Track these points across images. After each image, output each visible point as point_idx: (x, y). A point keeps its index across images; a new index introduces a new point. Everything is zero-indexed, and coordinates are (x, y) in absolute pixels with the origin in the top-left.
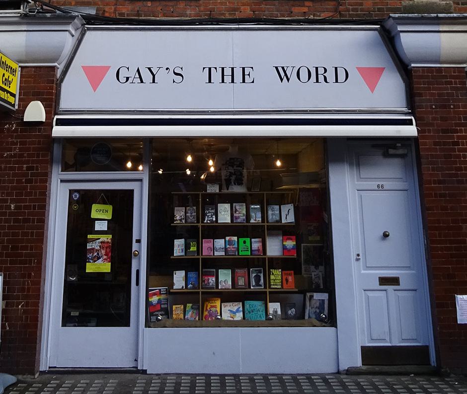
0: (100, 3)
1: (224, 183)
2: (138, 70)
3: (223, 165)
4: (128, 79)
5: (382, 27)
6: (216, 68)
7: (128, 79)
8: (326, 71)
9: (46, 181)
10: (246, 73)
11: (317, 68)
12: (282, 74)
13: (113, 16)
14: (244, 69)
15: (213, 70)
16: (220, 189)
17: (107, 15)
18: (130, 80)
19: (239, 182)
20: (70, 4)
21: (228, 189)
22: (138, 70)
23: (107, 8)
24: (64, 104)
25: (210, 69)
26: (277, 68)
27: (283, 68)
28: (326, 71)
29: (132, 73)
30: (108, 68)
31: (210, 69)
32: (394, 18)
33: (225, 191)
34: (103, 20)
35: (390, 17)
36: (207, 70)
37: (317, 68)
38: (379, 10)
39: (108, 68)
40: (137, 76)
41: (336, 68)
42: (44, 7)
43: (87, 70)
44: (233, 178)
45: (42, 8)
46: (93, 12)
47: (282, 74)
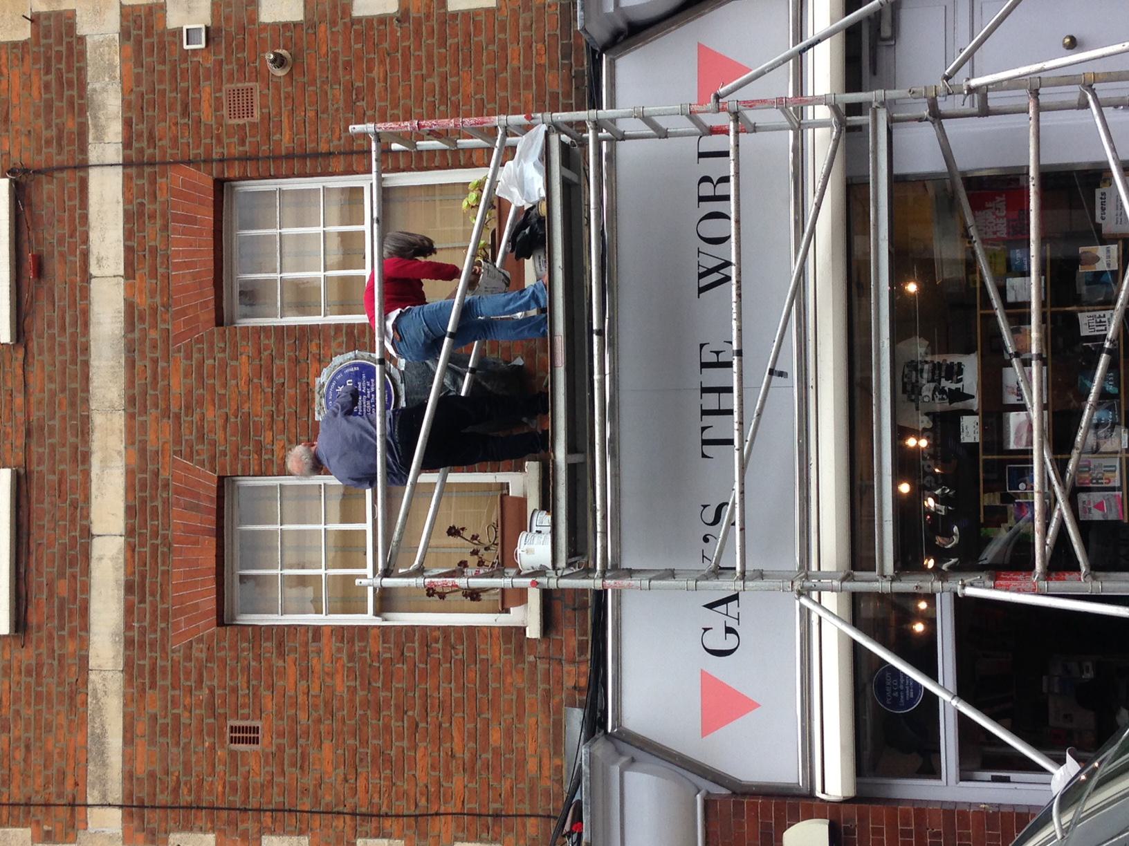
0: (557, 699)
1: (959, 405)
2: (711, 606)
3: (917, 409)
4: (729, 630)
5: (606, 48)
6: (703, 429)
7: (729, 630)
8: (706, 179)
9: (963, 815)
10: (713, 358)
11: (702, 199)
12: (715, 277)
13: (586, 668)
14: (704, 365)
15: (708, 435)
16: (970, 412)
17: (583, 682)
18: (732, 624)
19: (955, 372)
20: (559, 769)
21: (973, 397)
22: (711, 606)
23: (569, 683)
24: (786, 772)
25: (705, 442)
26: (702, 290)
27: (701, 276)
28: (706, 179)
29: (717, 619)
30: (705, 676)
31: (705, 442)
32: (586, 20)
33: (975, 404)
34: (596, 691)
35: (584, 29)
36: (709, 450)
37: (702, 199)
38: (566, 56)
39: (705, 676)
40: (722, 608)
41: (701, 155)
42: (567, 828)
43: (710, 723)
44: (947, 385)
45: (569, 834)
46: (575, 718)
47: (715, 277)
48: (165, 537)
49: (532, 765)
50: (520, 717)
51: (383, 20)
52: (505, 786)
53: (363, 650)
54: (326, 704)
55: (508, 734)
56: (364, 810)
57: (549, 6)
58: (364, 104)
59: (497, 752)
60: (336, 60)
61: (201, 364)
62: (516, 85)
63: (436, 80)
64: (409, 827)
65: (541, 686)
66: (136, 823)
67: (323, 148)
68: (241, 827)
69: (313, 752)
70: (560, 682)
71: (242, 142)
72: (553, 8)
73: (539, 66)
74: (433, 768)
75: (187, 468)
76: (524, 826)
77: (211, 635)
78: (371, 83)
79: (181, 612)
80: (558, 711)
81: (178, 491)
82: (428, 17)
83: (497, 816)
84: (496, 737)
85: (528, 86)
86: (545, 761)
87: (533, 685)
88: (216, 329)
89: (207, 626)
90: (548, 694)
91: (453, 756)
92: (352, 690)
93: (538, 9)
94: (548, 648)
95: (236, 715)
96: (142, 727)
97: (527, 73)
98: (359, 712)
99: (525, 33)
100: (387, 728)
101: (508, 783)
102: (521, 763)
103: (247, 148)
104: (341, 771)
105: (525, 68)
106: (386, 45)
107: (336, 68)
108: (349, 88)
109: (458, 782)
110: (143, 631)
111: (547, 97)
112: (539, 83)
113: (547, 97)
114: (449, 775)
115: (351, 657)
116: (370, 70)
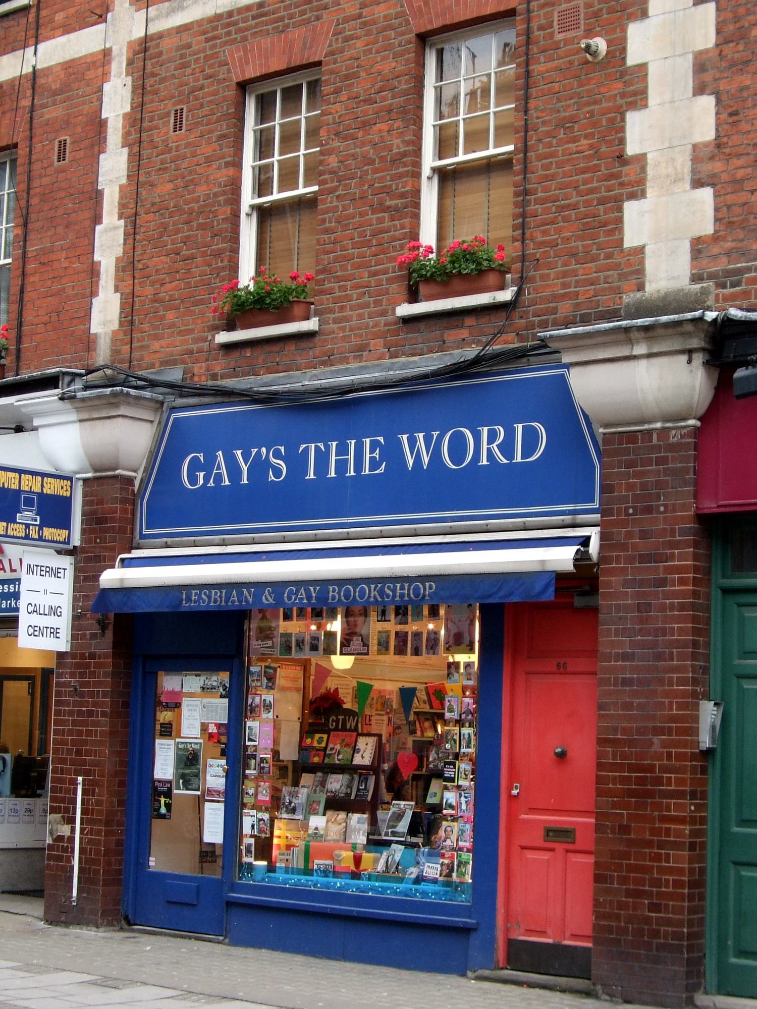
48: (287, 26)
49: (156, 345)
50: (180, 333)
51: (622, 141)
52: (146, 326)
53: (219, 202)
54: (192, 181)
55: (172, 325)
56: (138, 222)
57: (621, 298)
58: (562, 136)
59: (163, 318)
60: (596, 102)
61: (391, 28)
62: (565, 274)
63: (574, 199)
64: (128, 257)
65: (195, 347)
66: (137, 48)
67: (532, 103)
68: (132, 129)
69: (167, 176)
70: (197, 361)
71: (541, 28)
72: (618, 302)
73: (577, 294)
74: (157, 271)
75: (328, 33)
76: (126, 344)
77: (231, 80)
78: (575, 140)
79: (245, 52)
80: (183, 362)
81: (315, 27)
82: (622, 185)
83: (132, 323)
84: (171, 316)
85: (564, 286)
86: (158, 355)
87: (196, 341)
88: (414, 35)
89: (237, 76)
90: (190, 352)
91: (162, 284)
92: (197, 200)
93: (619, 288)
94: (215, 350)
95: (189, 111)
96: (186, 38)
97: (573, 284)
98: (186, 207)
99: (602, 278)
100: (178, 231)
101: (147, 329)
102: (157, 337)
103: (537, 33)
104: (157, 200)
105: (577, 281)
106: (604, 149)
107: (588, 104)
108: (573, 120)
109: (149, 290)
110: (235, 23)
111: (554, 305)
112: (564, 296)
113: (554, 305)
114: (152, 284)
115: (216, 195)
116: (586, 137)
